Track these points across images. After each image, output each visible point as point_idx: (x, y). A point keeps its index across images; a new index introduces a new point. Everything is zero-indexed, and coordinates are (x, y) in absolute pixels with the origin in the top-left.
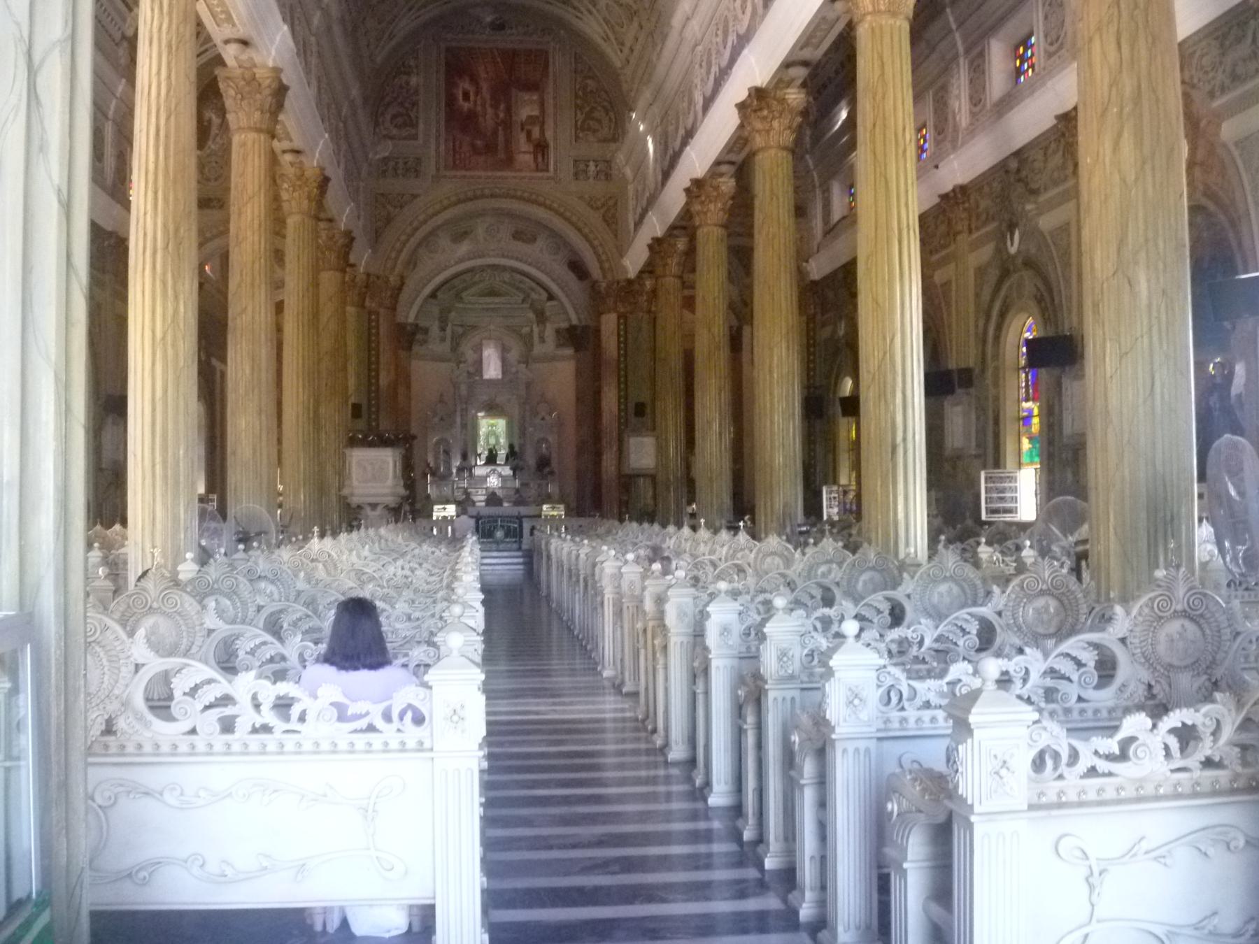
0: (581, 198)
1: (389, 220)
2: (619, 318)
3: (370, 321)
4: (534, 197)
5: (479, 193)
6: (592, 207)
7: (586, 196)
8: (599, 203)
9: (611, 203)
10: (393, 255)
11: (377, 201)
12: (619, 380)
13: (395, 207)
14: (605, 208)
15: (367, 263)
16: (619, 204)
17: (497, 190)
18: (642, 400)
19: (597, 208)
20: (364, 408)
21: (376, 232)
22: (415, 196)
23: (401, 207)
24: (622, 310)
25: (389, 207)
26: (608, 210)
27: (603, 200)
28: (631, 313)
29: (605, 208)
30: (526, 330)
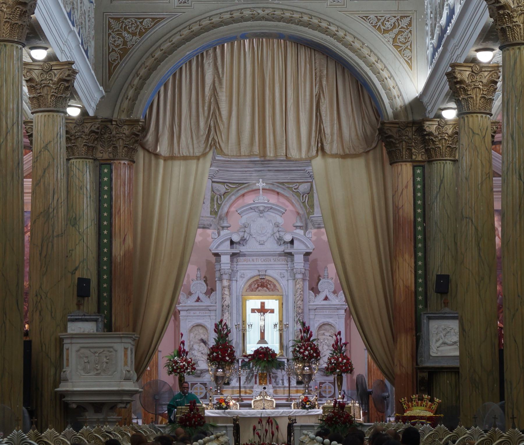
0: (366, 18)
1: (125, 51)
2: (414, 167)
3: (100, 176)
4: (306, 18)
5: (236, 15)
6: (379, 29)
7: (372, 16)
8: (388, 25)
9: (404, 23)
10: (131, 93)
11: (110, 28)
12: (415, 246)
13: (134, 34)
14: (396, 31)
15: (99, 106)
16: (414, 23)
17: (260, 11)
18: (445, 272)
19: (386, 31)
20: (94, 284)
21: (110, 64)
22: (156, 21)
23: (141, 34)
24: (419, 158)
25: (125, 34)
26: (400, 32)
27: (394, 20)
28: (430, 162)
29: (396, 31)
30: (303, 188)
